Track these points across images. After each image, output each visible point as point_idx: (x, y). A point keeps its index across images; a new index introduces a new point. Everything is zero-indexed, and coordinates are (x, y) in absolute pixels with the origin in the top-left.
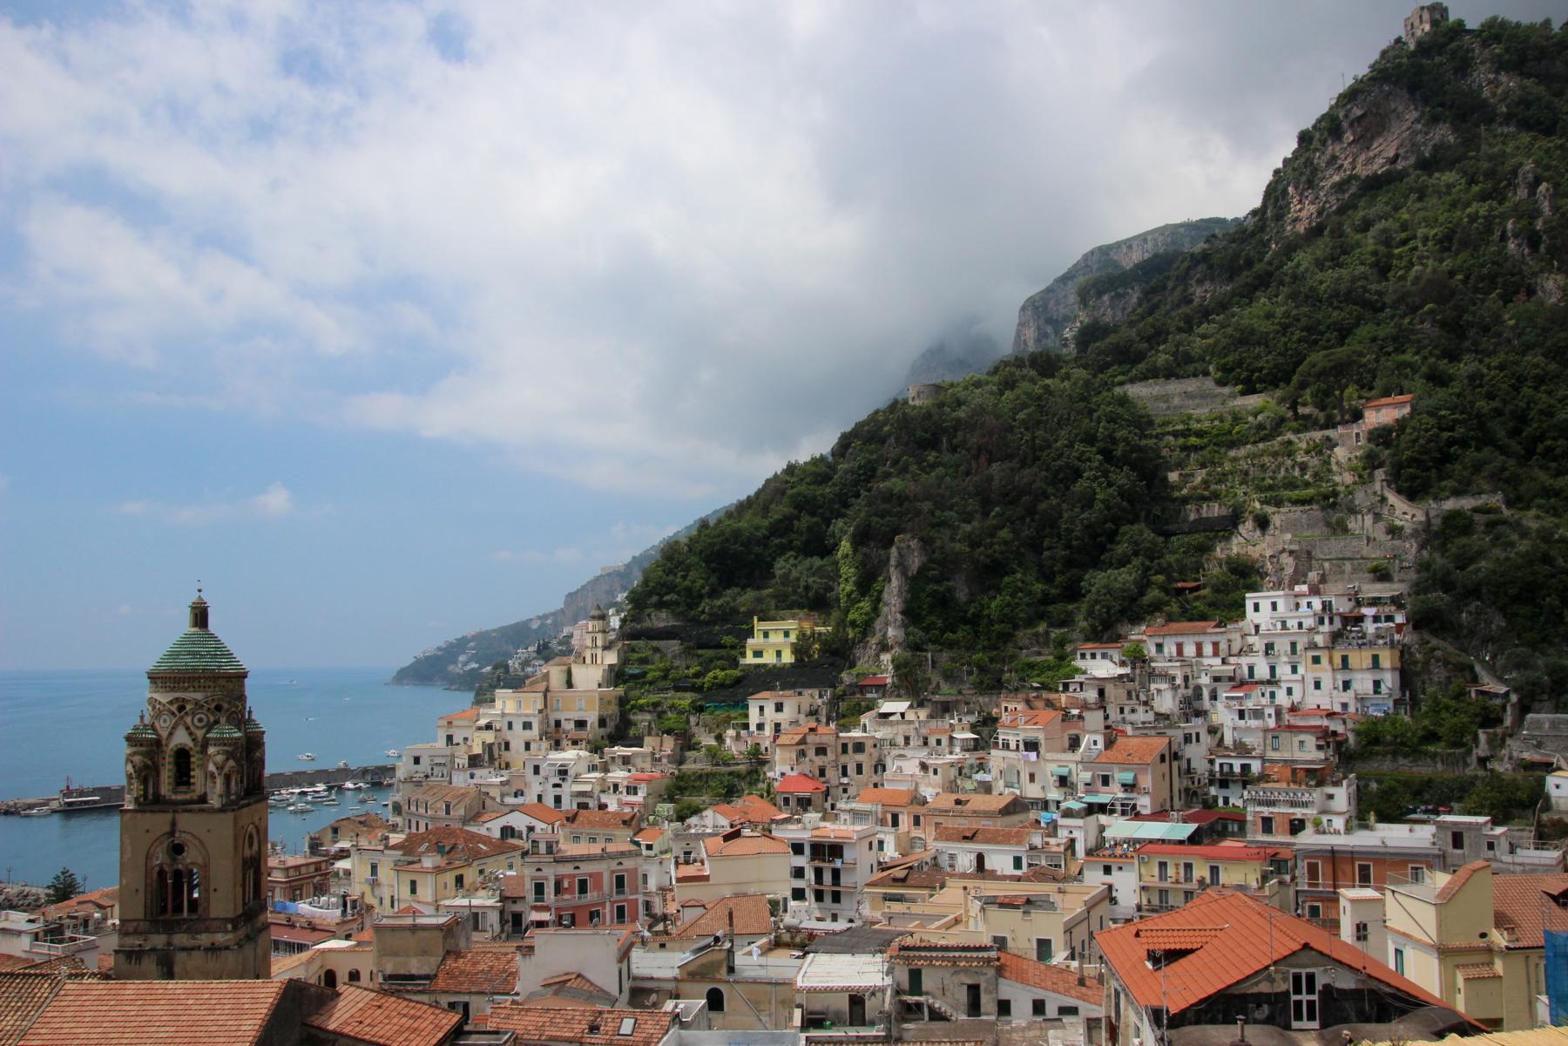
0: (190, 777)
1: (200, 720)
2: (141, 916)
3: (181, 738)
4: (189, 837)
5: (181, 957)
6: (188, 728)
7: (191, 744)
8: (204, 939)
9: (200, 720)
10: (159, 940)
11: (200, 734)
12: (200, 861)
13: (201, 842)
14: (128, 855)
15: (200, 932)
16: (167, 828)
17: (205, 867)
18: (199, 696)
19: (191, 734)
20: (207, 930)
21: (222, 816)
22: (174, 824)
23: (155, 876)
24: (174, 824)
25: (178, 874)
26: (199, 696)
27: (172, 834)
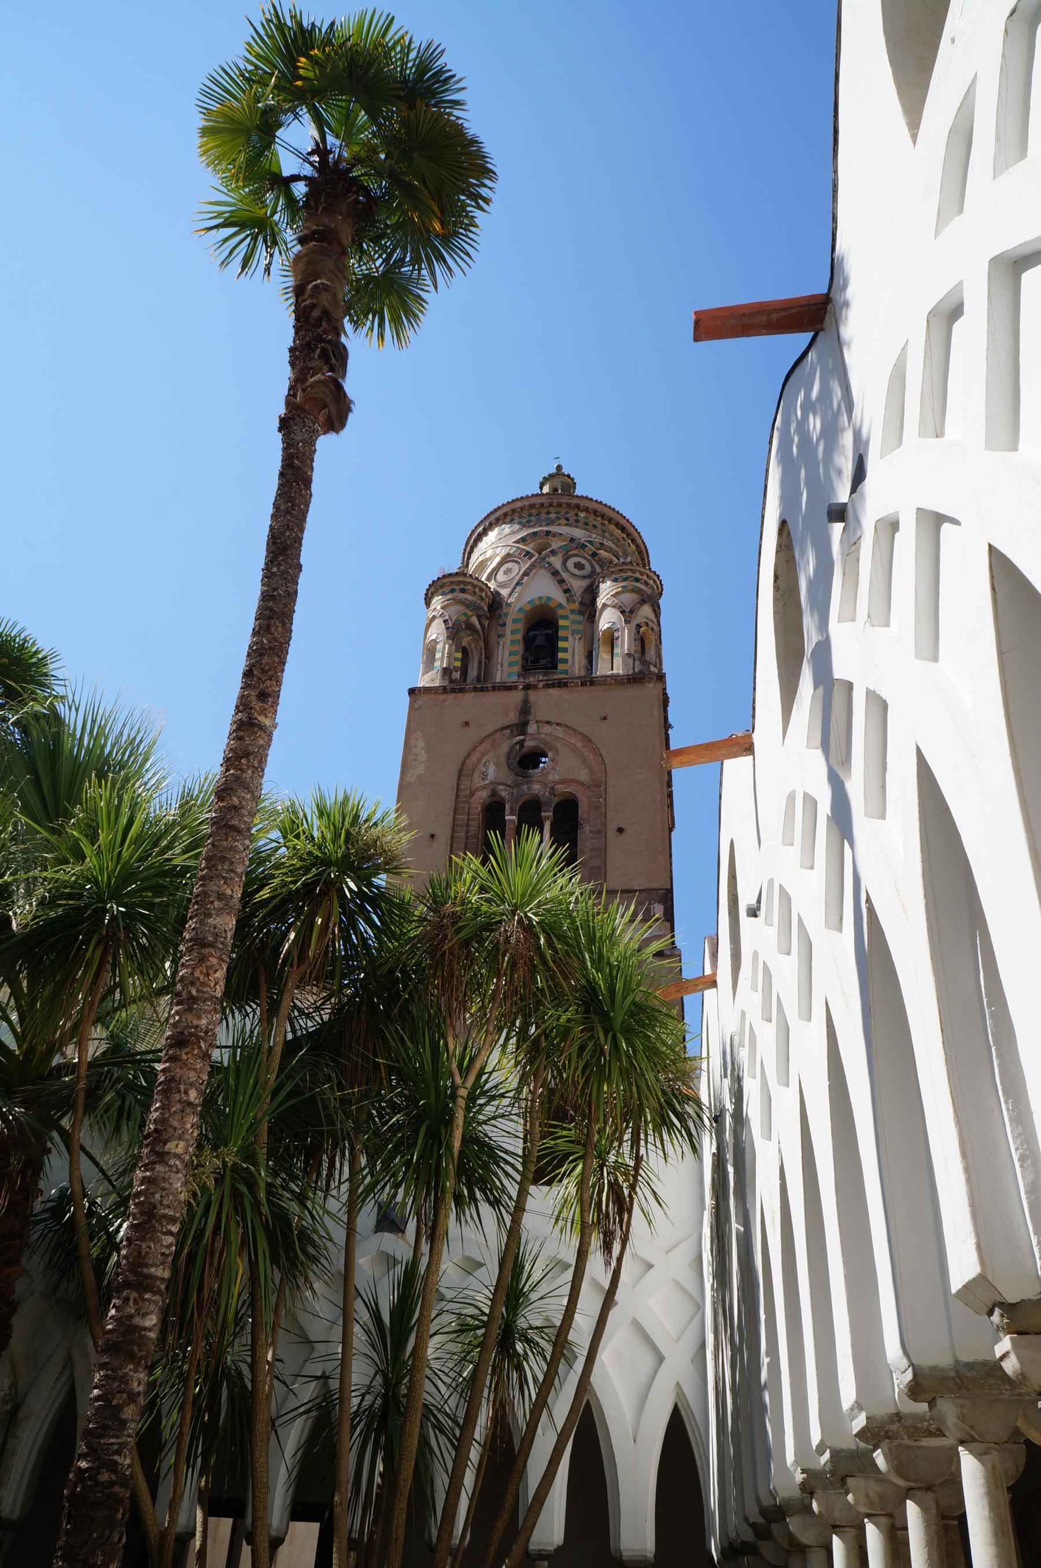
1: (579, 566)
3: (543, 588)
4: (559, 732)
6: (555, 573)
7: (558, 596)
11: (578, 586)
12: (583, 776)
13: (587, 740)
14: (420, 769)
16: (513, 718)
17: (598, 785)
18: (578, 533)
19: (561, 582)
21: (634, 691)
22: (525, 709)
23: (477, 809)
24: (525, 709)
26: (578, 533)
27: (521, 727)
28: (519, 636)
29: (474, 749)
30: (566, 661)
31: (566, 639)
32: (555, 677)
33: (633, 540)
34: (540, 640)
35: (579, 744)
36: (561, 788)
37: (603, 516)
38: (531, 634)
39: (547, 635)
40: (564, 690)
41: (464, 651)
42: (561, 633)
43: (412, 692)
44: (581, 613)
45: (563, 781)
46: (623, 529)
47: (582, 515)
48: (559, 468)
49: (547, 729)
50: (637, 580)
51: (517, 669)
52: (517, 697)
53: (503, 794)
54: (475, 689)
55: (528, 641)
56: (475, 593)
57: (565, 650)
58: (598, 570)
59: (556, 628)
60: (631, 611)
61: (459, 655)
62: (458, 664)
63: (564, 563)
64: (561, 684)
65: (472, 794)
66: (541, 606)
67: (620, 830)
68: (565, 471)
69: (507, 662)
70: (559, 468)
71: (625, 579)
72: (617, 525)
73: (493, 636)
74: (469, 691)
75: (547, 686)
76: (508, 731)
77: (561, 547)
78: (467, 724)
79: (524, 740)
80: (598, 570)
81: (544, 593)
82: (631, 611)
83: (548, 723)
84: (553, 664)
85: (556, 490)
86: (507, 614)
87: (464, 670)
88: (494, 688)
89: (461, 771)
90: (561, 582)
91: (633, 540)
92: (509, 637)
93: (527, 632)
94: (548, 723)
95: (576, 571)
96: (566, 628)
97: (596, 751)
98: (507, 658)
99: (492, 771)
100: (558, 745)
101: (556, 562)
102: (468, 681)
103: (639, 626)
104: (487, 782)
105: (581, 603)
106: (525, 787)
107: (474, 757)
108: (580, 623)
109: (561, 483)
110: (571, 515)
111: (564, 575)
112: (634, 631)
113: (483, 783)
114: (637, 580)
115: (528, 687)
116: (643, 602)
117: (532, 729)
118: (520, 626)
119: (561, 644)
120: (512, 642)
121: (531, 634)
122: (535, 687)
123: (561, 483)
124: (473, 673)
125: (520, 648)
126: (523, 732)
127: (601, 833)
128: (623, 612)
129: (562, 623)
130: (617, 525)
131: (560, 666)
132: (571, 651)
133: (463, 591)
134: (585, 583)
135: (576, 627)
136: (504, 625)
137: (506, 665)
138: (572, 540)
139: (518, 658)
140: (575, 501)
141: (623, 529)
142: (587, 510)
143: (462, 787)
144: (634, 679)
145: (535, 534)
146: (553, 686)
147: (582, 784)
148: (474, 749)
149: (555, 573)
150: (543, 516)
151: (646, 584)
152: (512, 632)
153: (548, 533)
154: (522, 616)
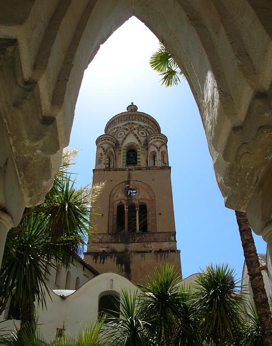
0: (136, 158)
1: (142, 133)
2: (105, 231)
3: (131, 140)
5: (135, 259)
6: (136, 135)
8: (154, 246)
9: (142, 133)
10: (120, 247)
11: (143, 139)
12: (148, 197)
13: (149, 187)
15: (148, 242)
16: (126, 179)
18: (142, 124)
19: (137, 138)
20: (156, 241)
21: (161, 171)
22: (129, 177)
24: (129, 177)
25: (132, 208)
26: (142, 124)
27: (128, 182)
28: (125, 154)
29: (114, 188)
30: (140, 162)
31: (139, 155)
32: (137, 167)
33: (157, 126)
34: (132, 155)
35: (146, 188)
36: (141, 201)
37: (148, 119)
38: (129, 153)
39: (134, 154)
40: (141, 171)
41: (109, 158)
42: (138, 153)
43: (93, 170)
44: (144, 148)
45: (142, 199)
46: (154, 122)
47: (142, 118)
48: (132, 103)
49: (136, 183)
50: (161, 138)
51: (125, 164)
52: (126, 173)
53: (124, 203)
54: (114, 170)
55: (128, 156)
56: (111, 141)
57: (139, 159)
58: (148, 135)
59: (136, 153)
60: (160, 148)
61: (108, 159)
62: (108, 162)
63: (138, 132)
64: (140, 169)
65: (114, 202)
66: (132, 145)
67: (160, 214)
68: (134, 104)
69: (121, 162)
70: (132, 103)
71: (157, 138)
72: (152, 121)
73: (117, 154)
74: (112, 171)
75: (135, 170)
76: (124, 183)
77: (137, 128)
78: (111, 181)
79: (129, 186)
80: (148, 135)
81: (133, 141)
82: (160, 148)
83: (137, 181)
84: (135, 163)
85: (132, 110)
86: (121, 147)
87: (109, 164)
88: (119, 170)
89: (110, 195)
90: (137, 138)
91: (157, 126)
92: (122, 154)
93: (128, 152)
94: (137, 181)
95: (142, 135)
96: (139, 152)
97: (151, 189)
98: (122, 161)
99: (120, 196)
100: (141, 189)
101: (136, 132)
102: (111, 167)
103: (162, 152)
104: (118, 198)
105: (144, 145)
106: (130, 201)
107: (114, 191)
108: (143, 150)
109: (132, 108)
110: (139, 118)
111: (138, 136)
112: (160, 154)
113: (117, 199)
114: (161, 138)
115: (130, 170)
116: (163, 145)
117: (131, 182)
118: (125, 151)
119: (138, 157)
120: (123, 156)
121: (129, 153)
122: (132, 170)
123: (132, 108)
124: (112, 165)
125: (125, 158)
126: (129, 184)
127: (154, 215)
128: (157, 148)
129: (138, 150)
130: (152, 121)
131: (138, 163)
132: (142, 159)
133: (108, 140)
134: (145, 138)
135: (142, 152)
136: (120, 150)
137: (121, 163)
138: (140, 126)
139: (125, 161)
140: (136, 113)
141: (154, 122)
142: (143, 116)
143: (111, 200)
144: (162, 168)
145: (129, 123)
146: (137, 170)
147: (148, 200)
148: (114, 188)
149: (136, 135)
150: (131, 118)
151: (163, 139)
152: (123, 153)
153: (133, 123)
154: (126, 148)
